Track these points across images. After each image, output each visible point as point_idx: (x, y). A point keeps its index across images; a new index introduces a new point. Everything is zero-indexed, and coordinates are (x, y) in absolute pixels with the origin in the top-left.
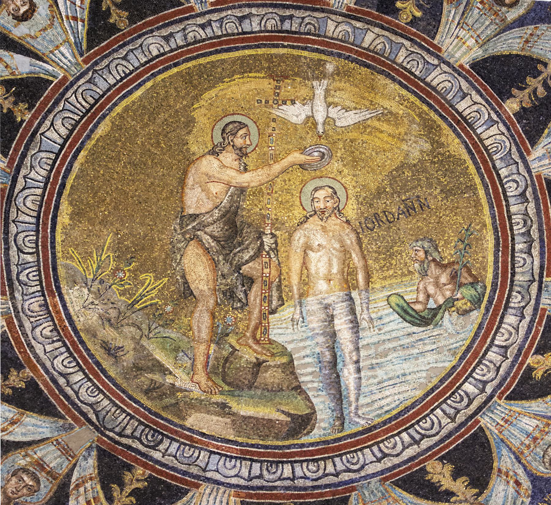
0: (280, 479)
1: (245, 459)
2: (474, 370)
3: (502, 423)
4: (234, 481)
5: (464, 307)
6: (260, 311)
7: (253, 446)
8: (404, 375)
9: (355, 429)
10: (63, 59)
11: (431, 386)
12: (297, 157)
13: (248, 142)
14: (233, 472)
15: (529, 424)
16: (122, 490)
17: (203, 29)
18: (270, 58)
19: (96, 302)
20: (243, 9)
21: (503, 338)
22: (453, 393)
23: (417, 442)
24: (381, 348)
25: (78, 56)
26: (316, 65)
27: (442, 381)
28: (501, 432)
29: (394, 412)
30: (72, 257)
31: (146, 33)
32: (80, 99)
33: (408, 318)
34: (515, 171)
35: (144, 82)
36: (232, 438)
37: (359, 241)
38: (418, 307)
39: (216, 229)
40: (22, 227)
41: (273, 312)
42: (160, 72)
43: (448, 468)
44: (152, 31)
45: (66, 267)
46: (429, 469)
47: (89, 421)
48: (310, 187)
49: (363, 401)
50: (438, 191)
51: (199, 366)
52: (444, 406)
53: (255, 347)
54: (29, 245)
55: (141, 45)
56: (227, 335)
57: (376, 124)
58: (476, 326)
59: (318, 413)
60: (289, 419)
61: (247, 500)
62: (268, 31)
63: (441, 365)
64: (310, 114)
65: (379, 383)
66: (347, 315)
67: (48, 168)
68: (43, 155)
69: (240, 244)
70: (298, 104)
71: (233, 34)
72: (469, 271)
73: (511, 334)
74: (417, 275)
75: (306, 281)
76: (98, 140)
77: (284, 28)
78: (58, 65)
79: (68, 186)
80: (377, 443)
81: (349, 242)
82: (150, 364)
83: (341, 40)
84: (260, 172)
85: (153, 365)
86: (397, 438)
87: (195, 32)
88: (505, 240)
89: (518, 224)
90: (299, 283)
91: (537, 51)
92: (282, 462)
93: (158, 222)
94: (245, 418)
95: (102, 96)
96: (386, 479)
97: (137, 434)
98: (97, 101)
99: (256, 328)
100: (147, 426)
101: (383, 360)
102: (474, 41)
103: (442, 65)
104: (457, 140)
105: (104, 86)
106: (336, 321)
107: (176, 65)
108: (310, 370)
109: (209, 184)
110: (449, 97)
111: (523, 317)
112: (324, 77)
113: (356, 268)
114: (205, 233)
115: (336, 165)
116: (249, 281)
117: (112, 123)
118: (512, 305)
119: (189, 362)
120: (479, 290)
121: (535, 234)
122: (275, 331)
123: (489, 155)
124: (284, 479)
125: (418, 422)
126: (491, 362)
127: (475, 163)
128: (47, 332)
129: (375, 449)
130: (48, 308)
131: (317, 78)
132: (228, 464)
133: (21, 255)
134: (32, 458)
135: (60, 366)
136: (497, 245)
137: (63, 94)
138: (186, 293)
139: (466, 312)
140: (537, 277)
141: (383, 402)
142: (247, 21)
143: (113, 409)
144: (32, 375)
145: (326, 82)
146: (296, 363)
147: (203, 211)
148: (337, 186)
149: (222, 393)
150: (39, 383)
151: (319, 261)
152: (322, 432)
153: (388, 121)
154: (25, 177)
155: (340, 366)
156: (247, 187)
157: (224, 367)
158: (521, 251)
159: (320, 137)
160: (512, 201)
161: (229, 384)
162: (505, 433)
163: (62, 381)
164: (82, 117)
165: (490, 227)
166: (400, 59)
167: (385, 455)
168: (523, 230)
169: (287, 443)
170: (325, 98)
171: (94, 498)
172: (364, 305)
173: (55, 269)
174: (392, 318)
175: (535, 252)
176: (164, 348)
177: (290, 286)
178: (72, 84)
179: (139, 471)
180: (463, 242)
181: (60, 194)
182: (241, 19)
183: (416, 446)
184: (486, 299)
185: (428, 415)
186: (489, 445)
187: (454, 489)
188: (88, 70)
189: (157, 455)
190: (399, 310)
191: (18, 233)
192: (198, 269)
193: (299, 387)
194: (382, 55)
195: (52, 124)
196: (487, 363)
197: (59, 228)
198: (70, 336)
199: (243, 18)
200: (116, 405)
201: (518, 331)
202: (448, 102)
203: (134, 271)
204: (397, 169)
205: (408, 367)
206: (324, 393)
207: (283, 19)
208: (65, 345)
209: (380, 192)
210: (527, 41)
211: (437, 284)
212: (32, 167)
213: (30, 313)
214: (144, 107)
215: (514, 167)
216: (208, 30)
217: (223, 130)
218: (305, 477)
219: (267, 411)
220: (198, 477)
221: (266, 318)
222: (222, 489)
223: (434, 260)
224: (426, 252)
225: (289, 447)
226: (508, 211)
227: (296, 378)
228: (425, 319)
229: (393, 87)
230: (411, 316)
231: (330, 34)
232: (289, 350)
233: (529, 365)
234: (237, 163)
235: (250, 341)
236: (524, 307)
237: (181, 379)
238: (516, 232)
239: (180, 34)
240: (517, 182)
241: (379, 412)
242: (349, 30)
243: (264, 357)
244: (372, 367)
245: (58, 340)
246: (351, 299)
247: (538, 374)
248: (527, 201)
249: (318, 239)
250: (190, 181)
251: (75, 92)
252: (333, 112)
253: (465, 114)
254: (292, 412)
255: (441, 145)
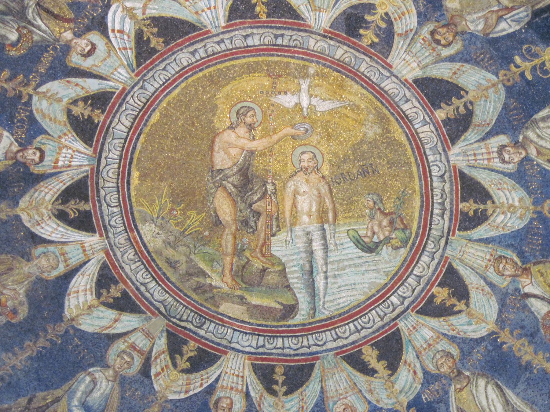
0: (275, 348)
1: (255, 334)
2: (398, 288)
3: (411, 328)
4: (248, 349)
5: (397, 244)
6: (266, 234)
7: (259, 325)
8: (354, 284)
9: (323, 317)
10: (121, 77)
11: (370, 294)
12: (289, 130)
13: (255, 120)
14: (247, 344)
15: (428, 334)
16: (182, 358)
17: (219, 45)
18: (268, 64)
19: (160, 232)
20: (247, 30)
21: (419, 270)
22: (384, 301)
23: (359, 331)
24: (341, 265)
25: (131, 73)
26: (301, 69)
27: (378, 292)
28: (410, 335)
29: (347, 308)
30: (143, 205)
31: (178, 51)
32: (137, 101)
33: (360, 246)
34: (439, 159)
35: (180, 83)
36: (247, 320)
37: (330, 190)
38: (367, 240)
39: (235, 179)
40: (107, 190)
41: (274, 235)
42: (190, 76)
43: (376, 353)
44: (182, 49)
45: (140, 211)
46: (364, 351)
47: (161, 313)
48: (300, 150)
49: (328, 298)
50: (385, 162)
51: (227, 271)
52: (377, 309)
53: (262, 258)
54: (113, 201)
55: (175, 60)
56: (244, 250)
57: (344, 111)
58: (402, 259)
59: (300, 304)
60: (282, 307)
61: (256, 362)
62: (266, 45)
63: (378, 281)
64: (298, 101)
65: (339, 287)
66: (321, 240)
67: (120, 149)
68: (116, 141)
69: (251, 190)
70: (289, 95)
71: (240, 48)
72: (402, 220)
73: (424, 269)
74: (367, 218)
75: (295, 215)
76: (152, 126)
77: (278, 43)
78: (118, 81)
79: (135, 160)
80: (335, 328)
81: (323, 191)
82: (196, 271)
83: (320, 53)
84: (264, 140)
85: (198, 272)
86: (347, 326)
87: (212, 47)
88: (428, 204)
89: (437, 195)
90: (290, 216)
91: (462, 81)
92: (277, 337)
93: (197, 175)
94: (256, 306)
95: (151, 96)
96: (338, 354)
97: (190, 319)
98: (148, 100)
99: (263, 246)
100: (196, 313)
101: (342, 272)
102: (416, 64)
103: (392, 77)
104: (400, 130)
105: (151, 89)
106: (314, 244)
107: (200, 71)
108: (296, 275)
109: (230, 148)
110: (397, 99)
111: (433, 259)
112: (308, 77)
113: (328, 209)
114: (228, 182)
115: (315, 138)
116: (258, 214)
117: (161, 113)
118: (427, 249)
119: (221, 269)
120: (407, 235)
121: (447, 205)
122: (275, 248)
123: (422, 144)
124: (277, 348)
125: (361, 317)
126: (409, 284)
127: (412, 148)
128: (131, 257)
129: (333, 332)
130: (130, 241)
131: (303, 77)
132: (244, 338)
133: (110, 208)
134: (128, 342)
135: (141, 278)
136: (422, 206)
137: (124, 99)
138: (217, 223)
139: (397, 248)
140: (445, 235)
141: (341, 301)
142: (250, 38)
143: (175, 304)
144: (124, 287)
145: (309, 80)
146: (287, 270)
147: (226, 167)
148: (316, 152)
149: (241, 289)
150: (129, 292)
151: (304, 202)
152: (302, 317)
153: (353, 110)
154: (106, 158)
155: (315, 274)
156: (255, 151)
157: (242, 271)
158: (437, 215)
159: (305, 117)
160: (435, 179)
161: (245, 283)
162: (412, 336)
163: (143, 289)
164: (139, 112)
165: (418, 193)
166: (362, 69)
167: (339, 337)
168: (440, 201)
169: (280, 324)
170: (309, 91)
171: (166, 366)
172: (332, 235)
173: (132, 213)
174: (349, 245)
175: (447, 217)
176: (204, 261)
177: (284, 218)
178: (129, 92)
179: (192, 343)
180: (400, 200)
181: (131, 163)
182: (246, 37)
183: (358, 334)
184: (411, 241)
185: (367, 314)
186: (402, 342)
187: (377, 369)
188: (139, 80)
189: (202, 333)
190: (355, 241)
191: (106, 195)
192: (224, 208)
193: (288, 287)
194: (349, 65)
195: (119, 121)
196: (407, 285)
197: (132, 187)
198: (146, 257)
199: (248, 36)
200: (177, 300)
201: (429, 267)
202: (396, 103)
203: (183, 210)
204: (358, 144)
205: (357, 279)
206: (304, 291)
207: (276, 37)
208: (143, 263)
209: (345, 159)
210: (455, 73)
211: (380, 225)
212: (109, 150)
213: (120, 246)
214: (181, 101)
215: (438, 156)
216: (222, 45)
217: (237, 113)
218: (290, 348)
219: (269, 301)
220: (226, 347)
221: (269, 239)
222: (241, 355)
223: (379, 209)
224: (375, 203)
225: (281, 327)
226: (432, 185)
227: (287, 280)
228: (371, 248)
229: (356, 87)
230: (362, 245)
231: (311, 48)
232: (283, 261)
233: (432, 293)
234: (248, 134)
235: (259, 255)
236: (435, 253)
237: (215, 280)
238: (435, 201)
239: (202, 49)
240: (439, 167)
241: (338, 307)
242: (326, 46)
243: (266, 266)
244: (335, 277)
245: (139, 261)
246: (324, 229)
247: (438, 301)
248: (445, 181)
249: (303, 188)
250: (216, 147)
251: (132, 97)
252: (314, 101)
253: (407, 113)
254: (284, 303)
255: (389, 132)
